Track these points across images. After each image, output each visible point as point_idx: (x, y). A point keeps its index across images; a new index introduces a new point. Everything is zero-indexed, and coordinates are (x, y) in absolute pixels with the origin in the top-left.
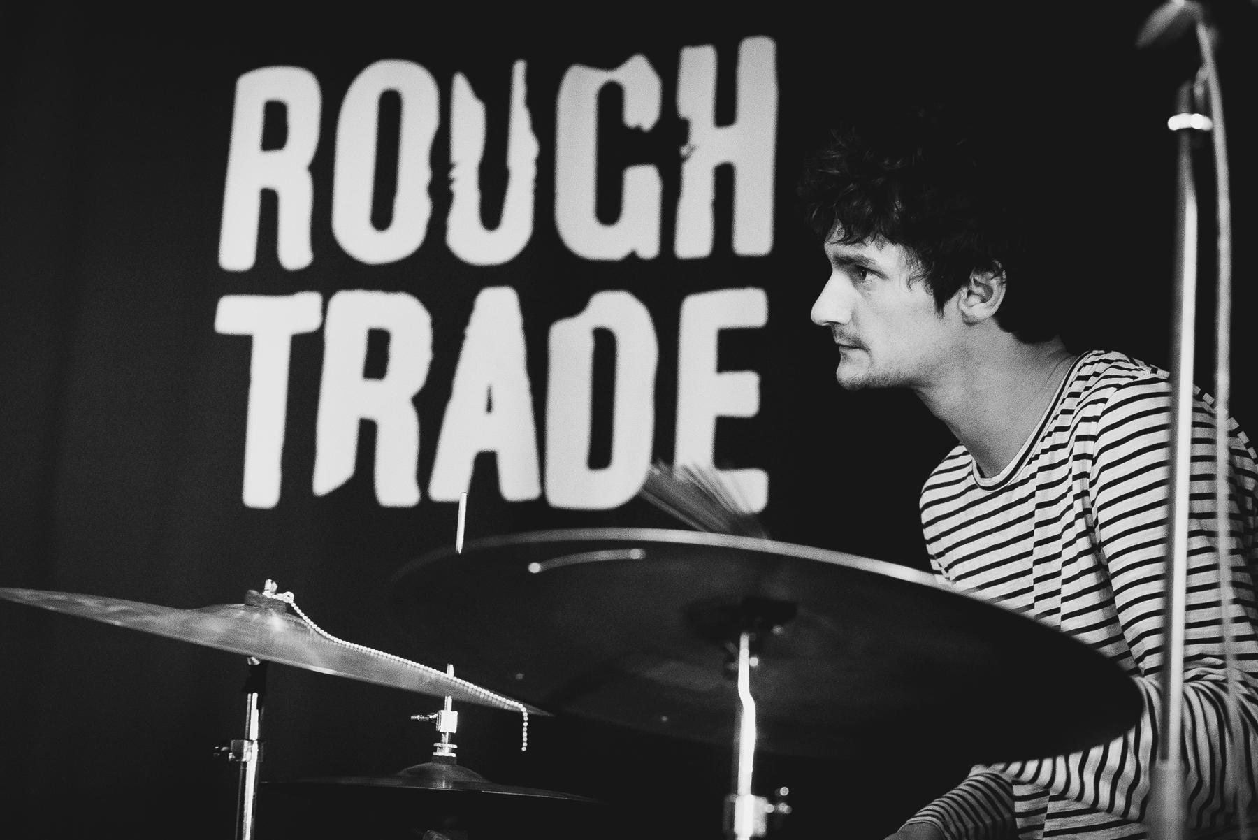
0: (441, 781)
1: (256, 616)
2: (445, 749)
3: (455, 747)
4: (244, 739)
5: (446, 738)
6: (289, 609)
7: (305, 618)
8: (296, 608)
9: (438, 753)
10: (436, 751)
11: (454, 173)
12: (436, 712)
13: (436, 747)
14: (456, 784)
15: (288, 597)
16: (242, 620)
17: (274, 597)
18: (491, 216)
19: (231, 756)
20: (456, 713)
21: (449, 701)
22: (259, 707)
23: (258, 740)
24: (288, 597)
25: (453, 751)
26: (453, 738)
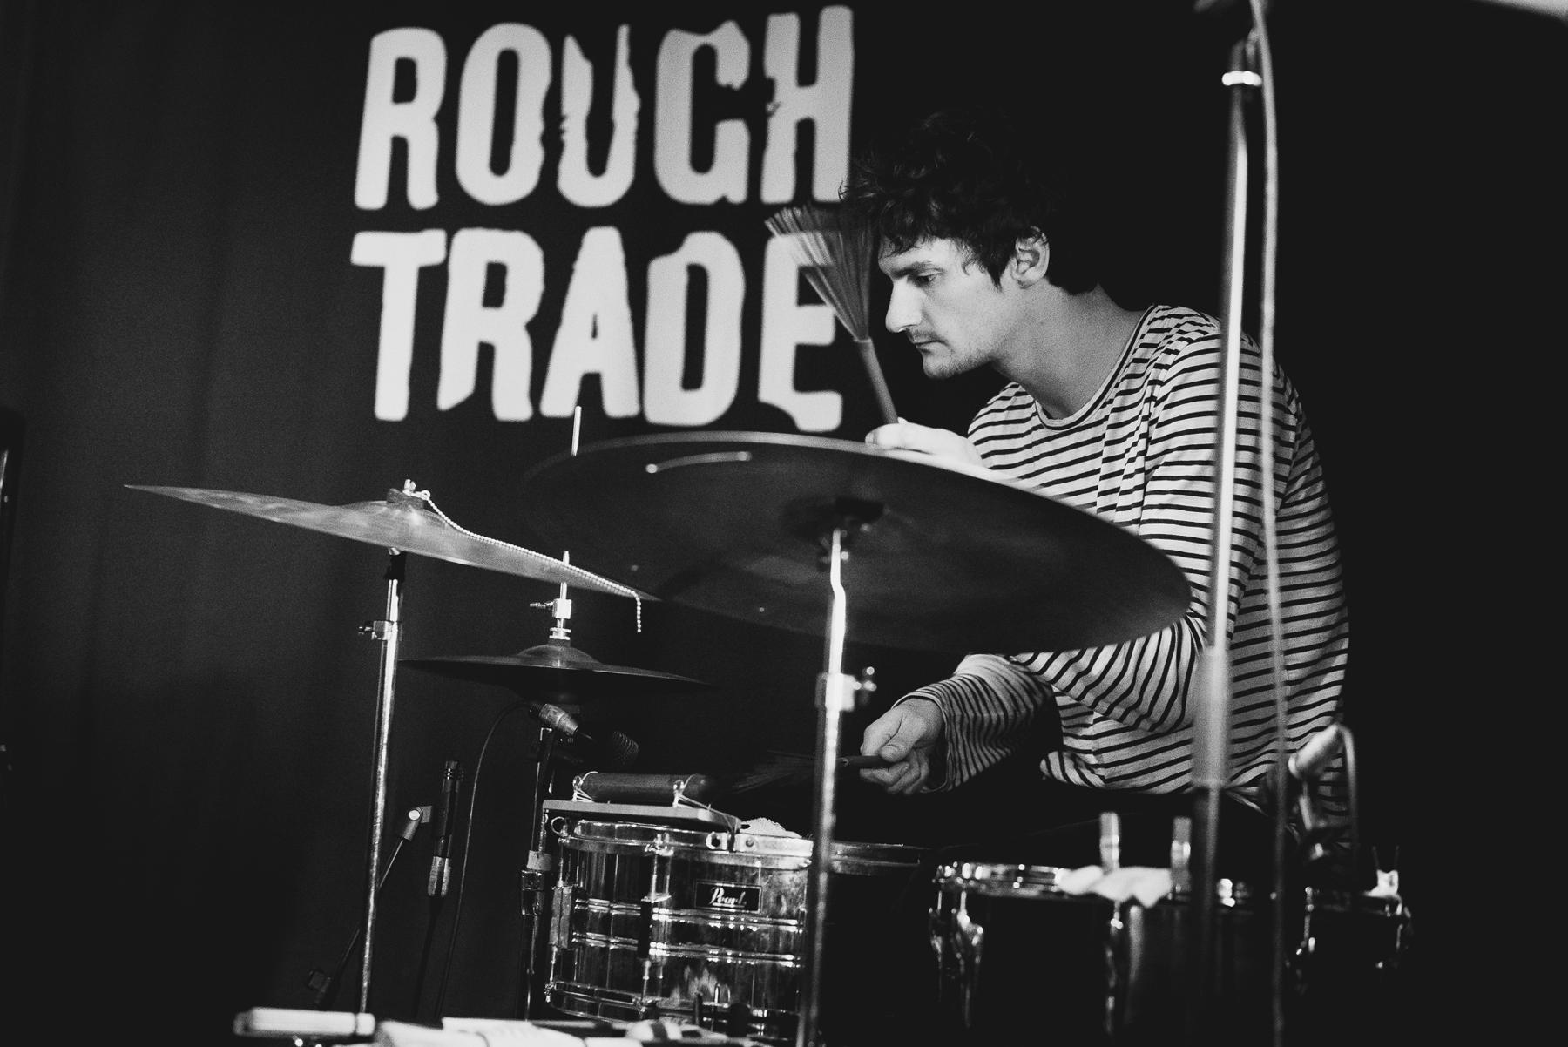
0: (557, 661)
1: (398, 512)
2: (560, 633)
3: (569, 631)
5: (560, 624)
6: (426, 506)
7: (441, 513)
8: (433, 505)
9: (554, 637)
11: (565, 125)
13: (552, 632)
14: (569, 663)
15: (425, 495)
16: (385, 516)
17: (413, 495)
18: (597, 163)
20: (570, 601)
21: (564, 588)
24: (425, 495)
25: (568, 634)
26: (567, 624)
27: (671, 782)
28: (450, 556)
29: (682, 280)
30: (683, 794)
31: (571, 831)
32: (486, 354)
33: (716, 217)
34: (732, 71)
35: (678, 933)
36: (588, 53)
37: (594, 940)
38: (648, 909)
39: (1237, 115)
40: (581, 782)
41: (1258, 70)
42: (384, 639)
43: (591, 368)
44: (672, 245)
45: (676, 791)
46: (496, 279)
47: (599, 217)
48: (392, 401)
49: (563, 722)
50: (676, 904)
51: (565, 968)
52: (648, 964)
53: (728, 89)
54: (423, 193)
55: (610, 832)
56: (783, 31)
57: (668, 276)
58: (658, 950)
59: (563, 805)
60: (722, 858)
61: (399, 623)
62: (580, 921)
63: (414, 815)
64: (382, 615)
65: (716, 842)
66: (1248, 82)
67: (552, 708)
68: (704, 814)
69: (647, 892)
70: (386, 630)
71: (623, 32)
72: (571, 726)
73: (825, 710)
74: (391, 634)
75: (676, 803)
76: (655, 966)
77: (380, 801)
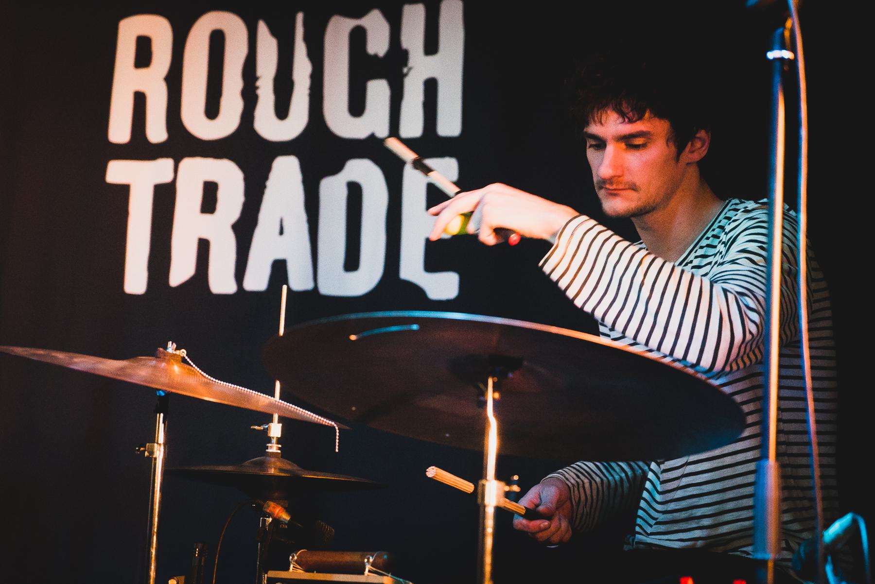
1: (163, 365)
2: (274, 448)
3: (280, 446)
4: (154, 442)
5: (274, 441)
7: (194, 366)
8: (188, 360)
9: (269, 450)
10: (268, 449)
11: (258, 83)
12: (267, 424)
14: (281, 470)
15: (183, 353)
16: (155, 367)
17: (174, 352)
18: (282, 111)
19: (146, 454)
20: (281, 425)
21: (276, 417)
22: (164, 422)
23: (164, 443)
24: (183, 353)
25: (279, 449)
26: (279, 441)
27: (363, 557)
28: (203, 396)
29: (343, 193)
30: (371, 566)
32: (204, 246)
36: (274, 32)
39: (777, 79)
40: (296, 558)
41: (793, 50)
42: (154, 456)
43: (280, 256)
44: (336, 168)
45: (367, 564)
46: (210, 192)
49: (280, 514)
53: (376, 56)
54: (157, 132)
61: (165, 444)
64: (153, 439)
66: (786, 57)
67: (272, 504)
70: (155, 450)
71: (300, 17)
73: (484, 506)
74: (159, 453)
75: (366, 572)
77: (152, 574)
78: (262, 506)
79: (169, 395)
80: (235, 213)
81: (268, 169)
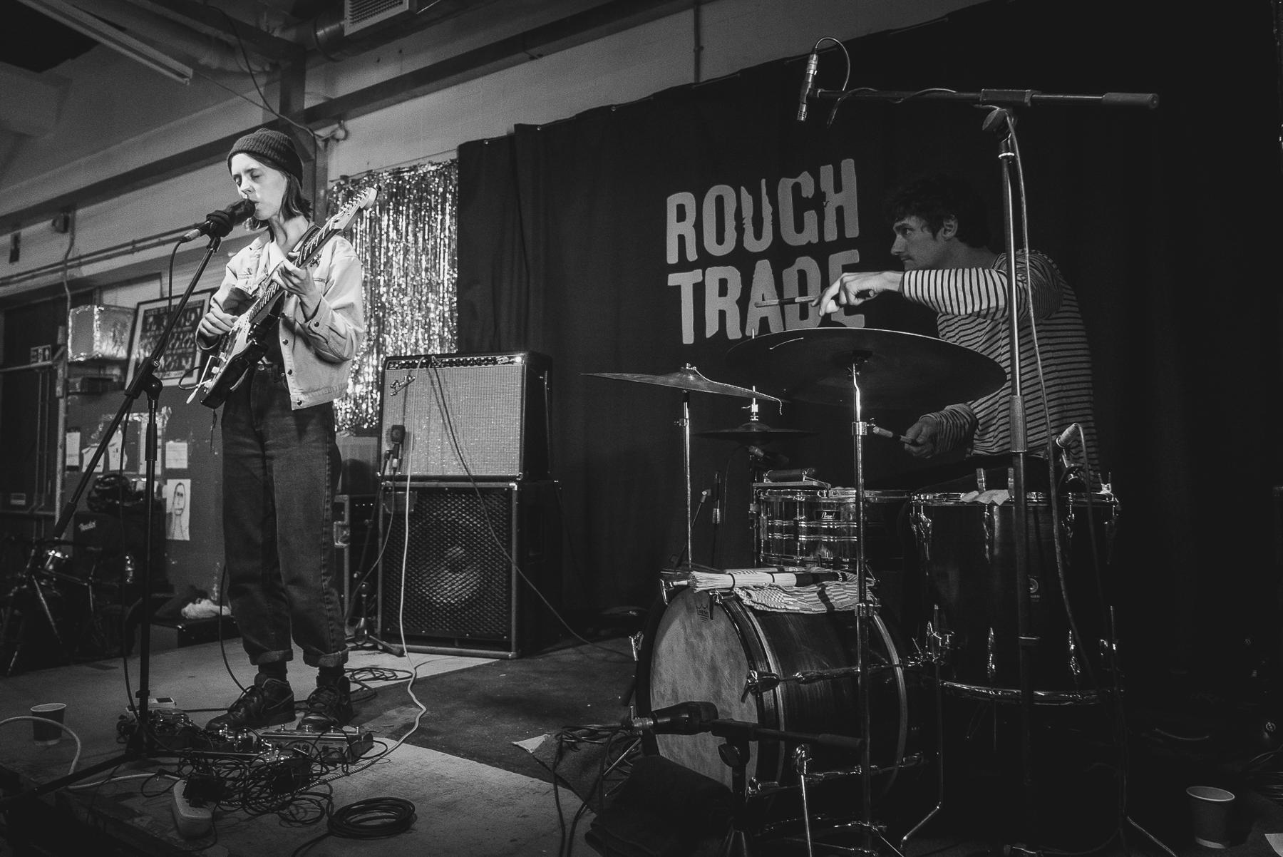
6: (695, 373)
24: (695, 368)
31: (764, 494)
32: (722, 314)
33: (808, 250)
34: (808, 191)
35: (810, 531)
37: (777, 536)
38: (796, 522)
47: (761, 256)
48: (688, 337)
50: (808, 519)
51: (767, 548)
52: (799, 544)
53: (807, 197)
55: (780, 494)
56: (827, 172)
57: (790, 275)
58: (803, 538)
59: (760, 485)
60: (824, 499)
62: (772, 529)
63: (704, 493)
65: (821, 494)
68: (815, 483)
69: (796, 515)
72: (761, 454)
76: (801, 544)
78: (748, 449)
79: (689, 392)
80: (738, 295)
81: (754, 268)
